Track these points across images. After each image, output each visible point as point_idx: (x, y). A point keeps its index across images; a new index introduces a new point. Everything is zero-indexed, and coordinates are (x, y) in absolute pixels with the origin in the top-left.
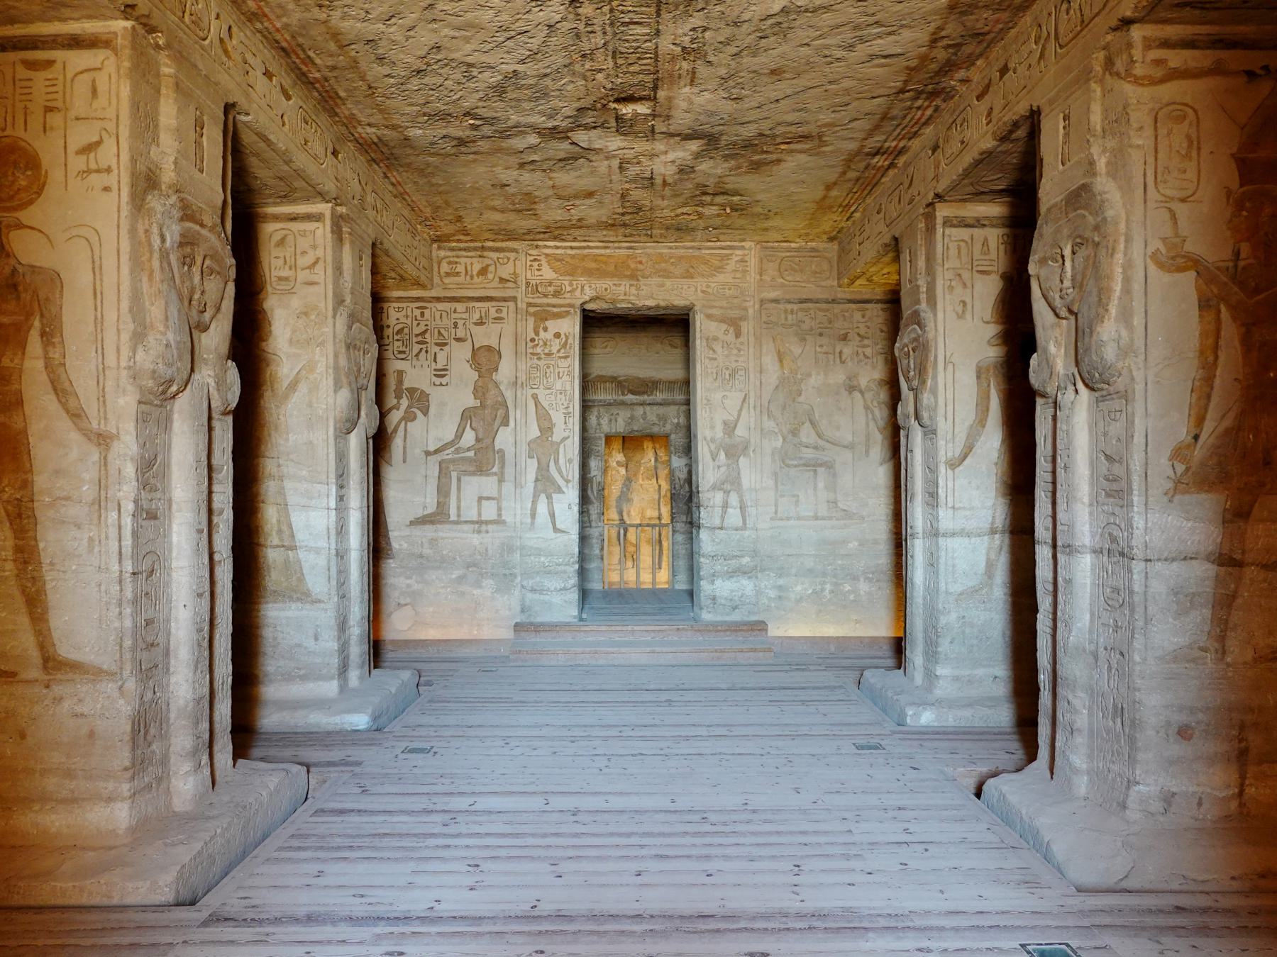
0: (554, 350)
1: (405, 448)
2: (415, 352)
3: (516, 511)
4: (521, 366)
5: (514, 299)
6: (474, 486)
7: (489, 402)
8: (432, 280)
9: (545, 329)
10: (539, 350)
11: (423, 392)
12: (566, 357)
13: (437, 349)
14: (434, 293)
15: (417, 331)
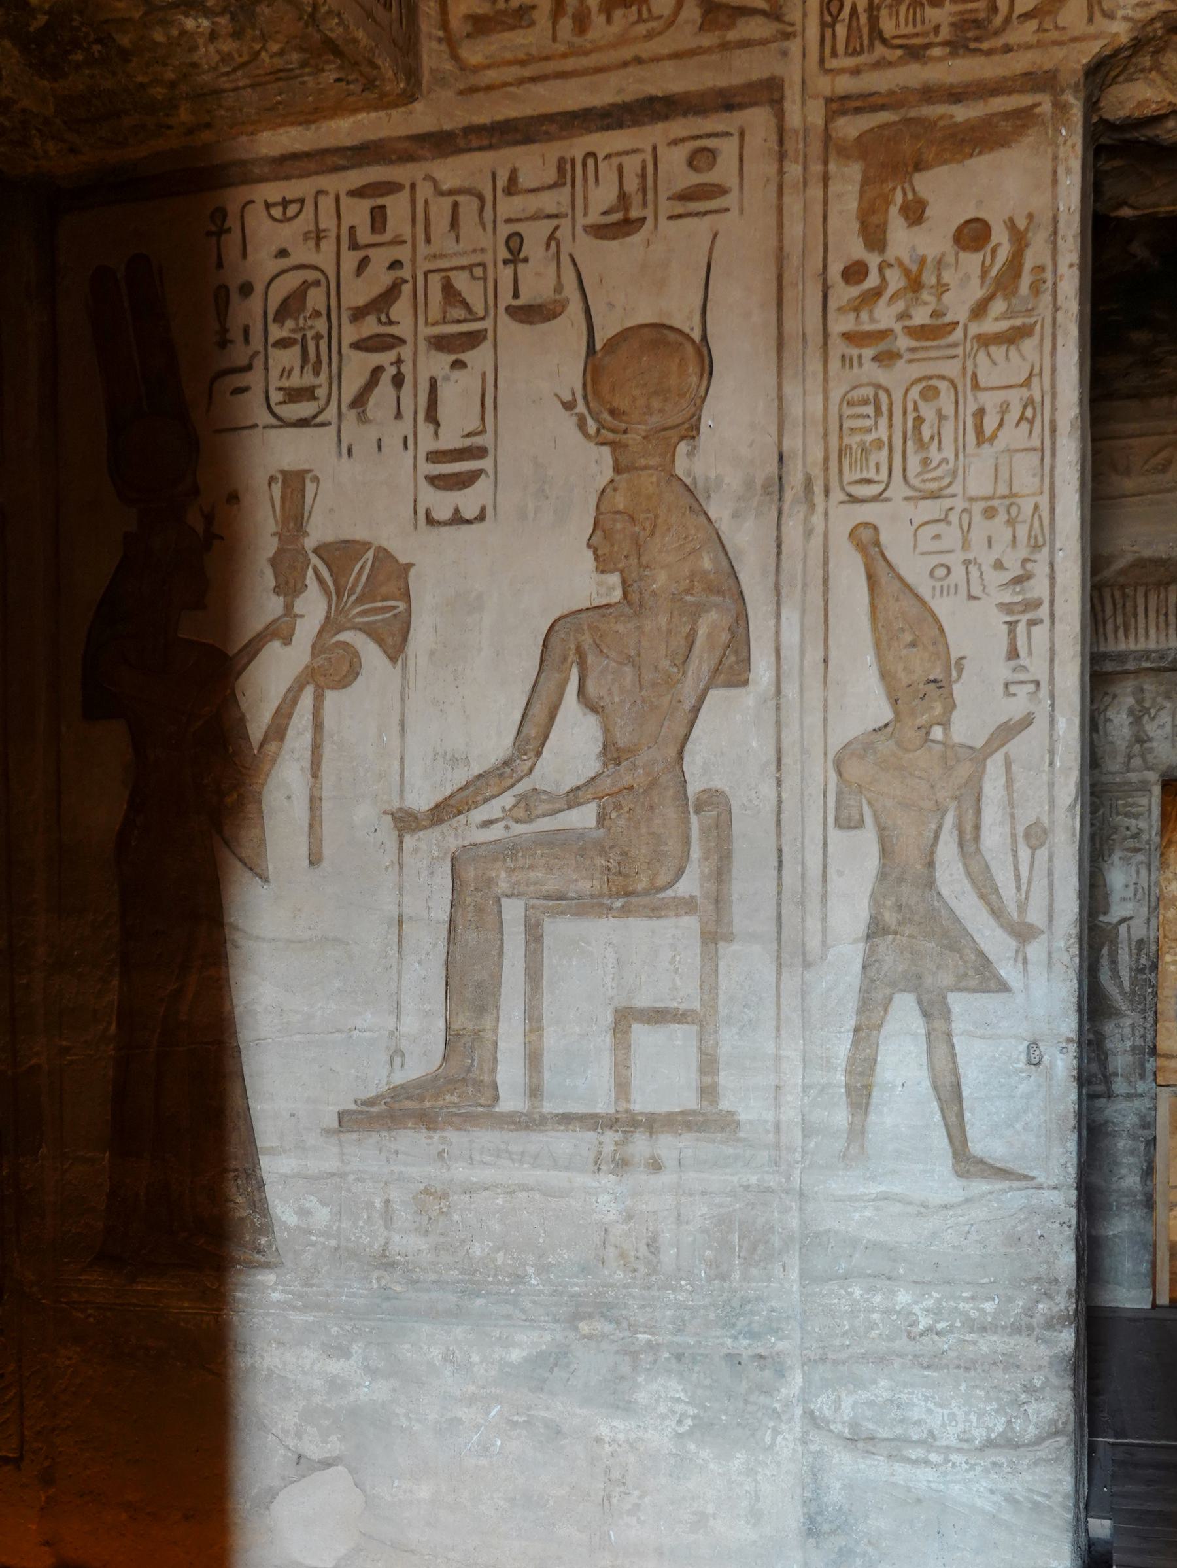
0: (958, 306)
1: (315, 802)
2: (351, 387)
3: (780, 1073)
4: (805, 402)
5: (769, 92)
6: (599, 960)
7: (660, 580)
8: (407, 47)
9: (915, 213)
10: (884, 316)
11: (382, 555)
12: (1013, 337)
13: (437, 364)
14: (422, 117)
15: (357, 293)
